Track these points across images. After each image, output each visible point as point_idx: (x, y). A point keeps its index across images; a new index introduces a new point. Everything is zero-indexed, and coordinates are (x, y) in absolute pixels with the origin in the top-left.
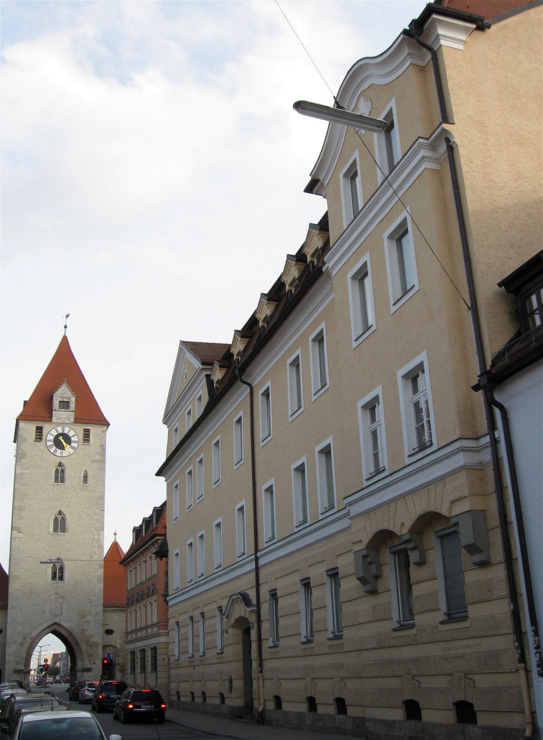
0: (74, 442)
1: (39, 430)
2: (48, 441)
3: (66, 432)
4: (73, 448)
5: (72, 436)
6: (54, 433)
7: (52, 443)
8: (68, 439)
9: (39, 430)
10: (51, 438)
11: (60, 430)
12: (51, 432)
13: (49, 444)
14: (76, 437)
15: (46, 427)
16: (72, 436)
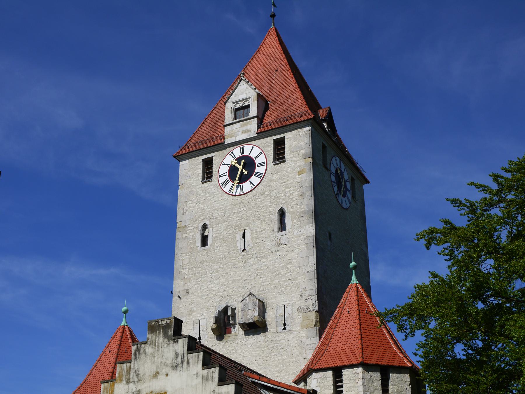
0: (261, 165)
1: (208, 164)
2: (221, 176)
3: (246, 153)
4: (259, 175)
5: (256, 158)
6: (230, 160)
7: (227, 177)
8: (249, 164)
9: (208, 164)
10: (225, 169)
11: (237, 152)
12: (223, 162)
13: (222, 180)
14: (263, 155)
15: (216, 156)
16: (256, 158)
